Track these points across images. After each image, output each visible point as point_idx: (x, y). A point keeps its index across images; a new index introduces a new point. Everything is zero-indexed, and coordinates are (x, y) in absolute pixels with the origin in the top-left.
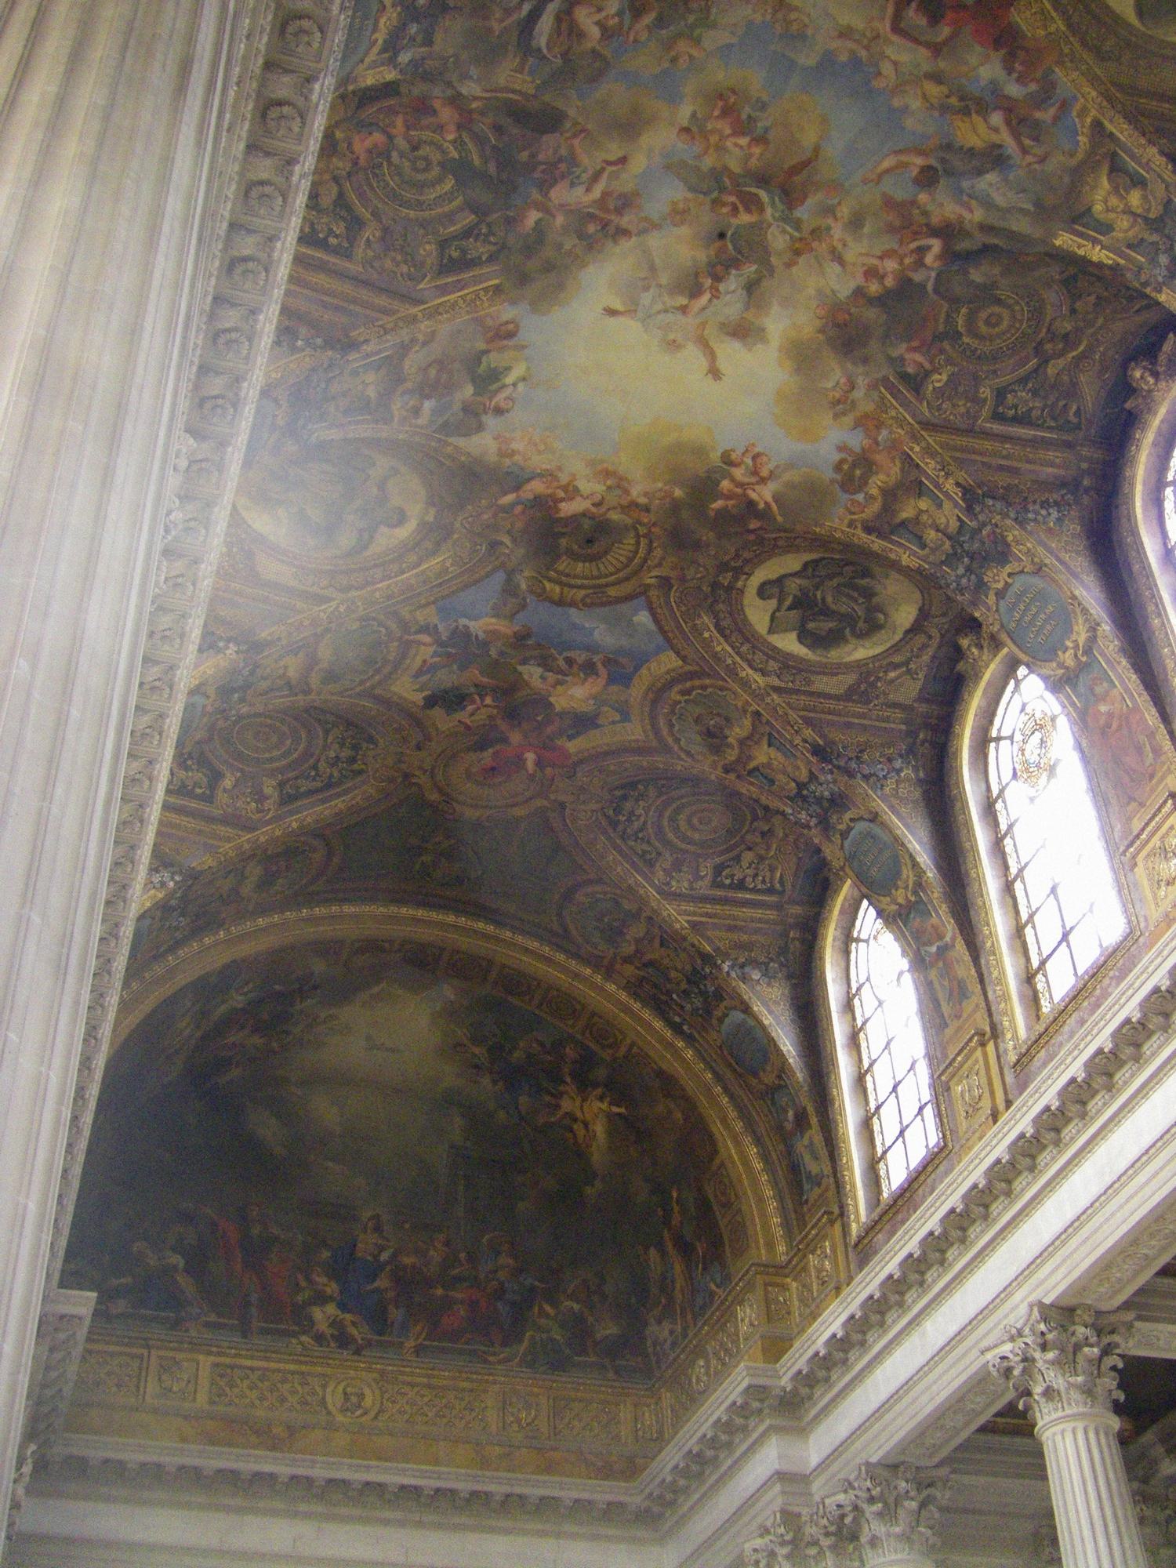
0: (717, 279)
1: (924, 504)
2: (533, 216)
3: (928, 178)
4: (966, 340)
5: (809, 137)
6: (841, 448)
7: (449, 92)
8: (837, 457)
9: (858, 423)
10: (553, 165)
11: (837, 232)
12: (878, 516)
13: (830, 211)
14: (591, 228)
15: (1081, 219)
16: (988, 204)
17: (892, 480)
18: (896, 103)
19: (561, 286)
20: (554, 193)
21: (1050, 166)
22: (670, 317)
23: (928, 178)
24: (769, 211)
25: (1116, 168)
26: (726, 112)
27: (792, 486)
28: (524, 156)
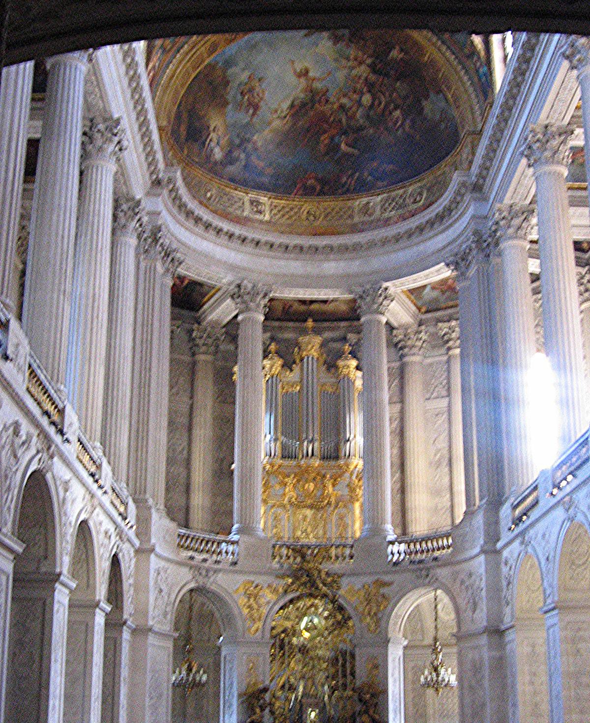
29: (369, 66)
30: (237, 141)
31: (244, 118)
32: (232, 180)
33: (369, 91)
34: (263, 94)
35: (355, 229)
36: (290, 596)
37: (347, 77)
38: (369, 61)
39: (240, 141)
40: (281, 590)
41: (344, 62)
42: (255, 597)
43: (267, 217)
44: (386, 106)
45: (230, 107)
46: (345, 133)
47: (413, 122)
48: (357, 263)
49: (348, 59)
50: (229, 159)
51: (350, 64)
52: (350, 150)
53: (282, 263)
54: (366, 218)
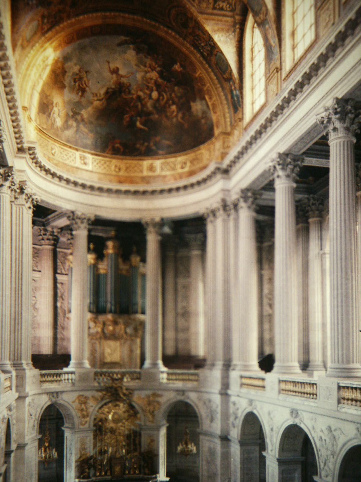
29: (158, 72)
30: (71, 114)
32: (68, 141)
33: (157, 90)
34: (88, 83)
36: (103, 402)
37: (143, 78)
38: (158, 69)
41: (142, 67)
46: (140, 116)
49: (145, 66)
50: (66, 126)
51: (146, 69)
52: (142, 127)
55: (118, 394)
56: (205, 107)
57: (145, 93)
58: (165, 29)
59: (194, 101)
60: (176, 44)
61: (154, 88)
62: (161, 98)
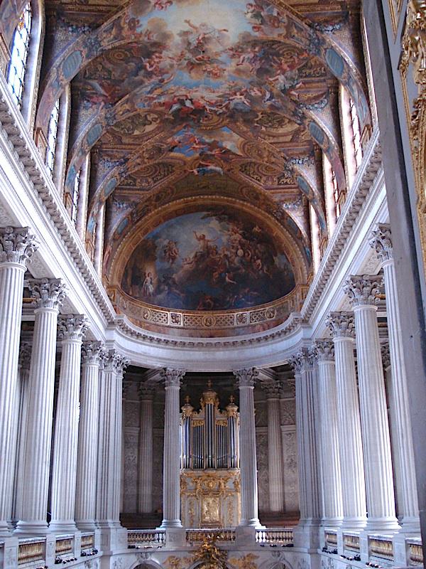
0: (199, 43)
1: (112, 36)
2: (257, 49)
3: (162, 81)
4: (123, 50)
5: (193, 74)
6: (141, 25)
7: (286, 75)
8: (141, 23)
9: (141, 33)
10: (255, 60)
11: (175, 62)
12: (120, 22)
13: (179, 65)
14: (240, 50)
15: (127, 102)
16: (146, 86)
17: (123, 31)
18: (177, 86)
19: (244, 38)
20: (253, 55)
21: (139, 100)
22: (208, 32)
23: (162, 81)
24: (194, 59)
25: (128, 110)
26: (216, 74)
27: (148, 7)
28: (263, 61)
31: (166, 265)
33: (242, 249)
35: (235, 331)
37: (228, 240)
39: (165, 279)
40: (192, 561)
42: (176, 565)
43: (182, 325)
44: (251, 258)
45: (158, 259)
47: (268, 267)
48: (236, 352)
49: (229, 231)
50: (158, 291)
51: (230, 233)
53: (191, 353)
54: (241, 324)
55: (210, 556)
56: (285, 261)
57: (231, 252)
58: (241, 202)
59: (276, 256)
60: (251, 211)
61: (239, 247)
62: (246, 254)
